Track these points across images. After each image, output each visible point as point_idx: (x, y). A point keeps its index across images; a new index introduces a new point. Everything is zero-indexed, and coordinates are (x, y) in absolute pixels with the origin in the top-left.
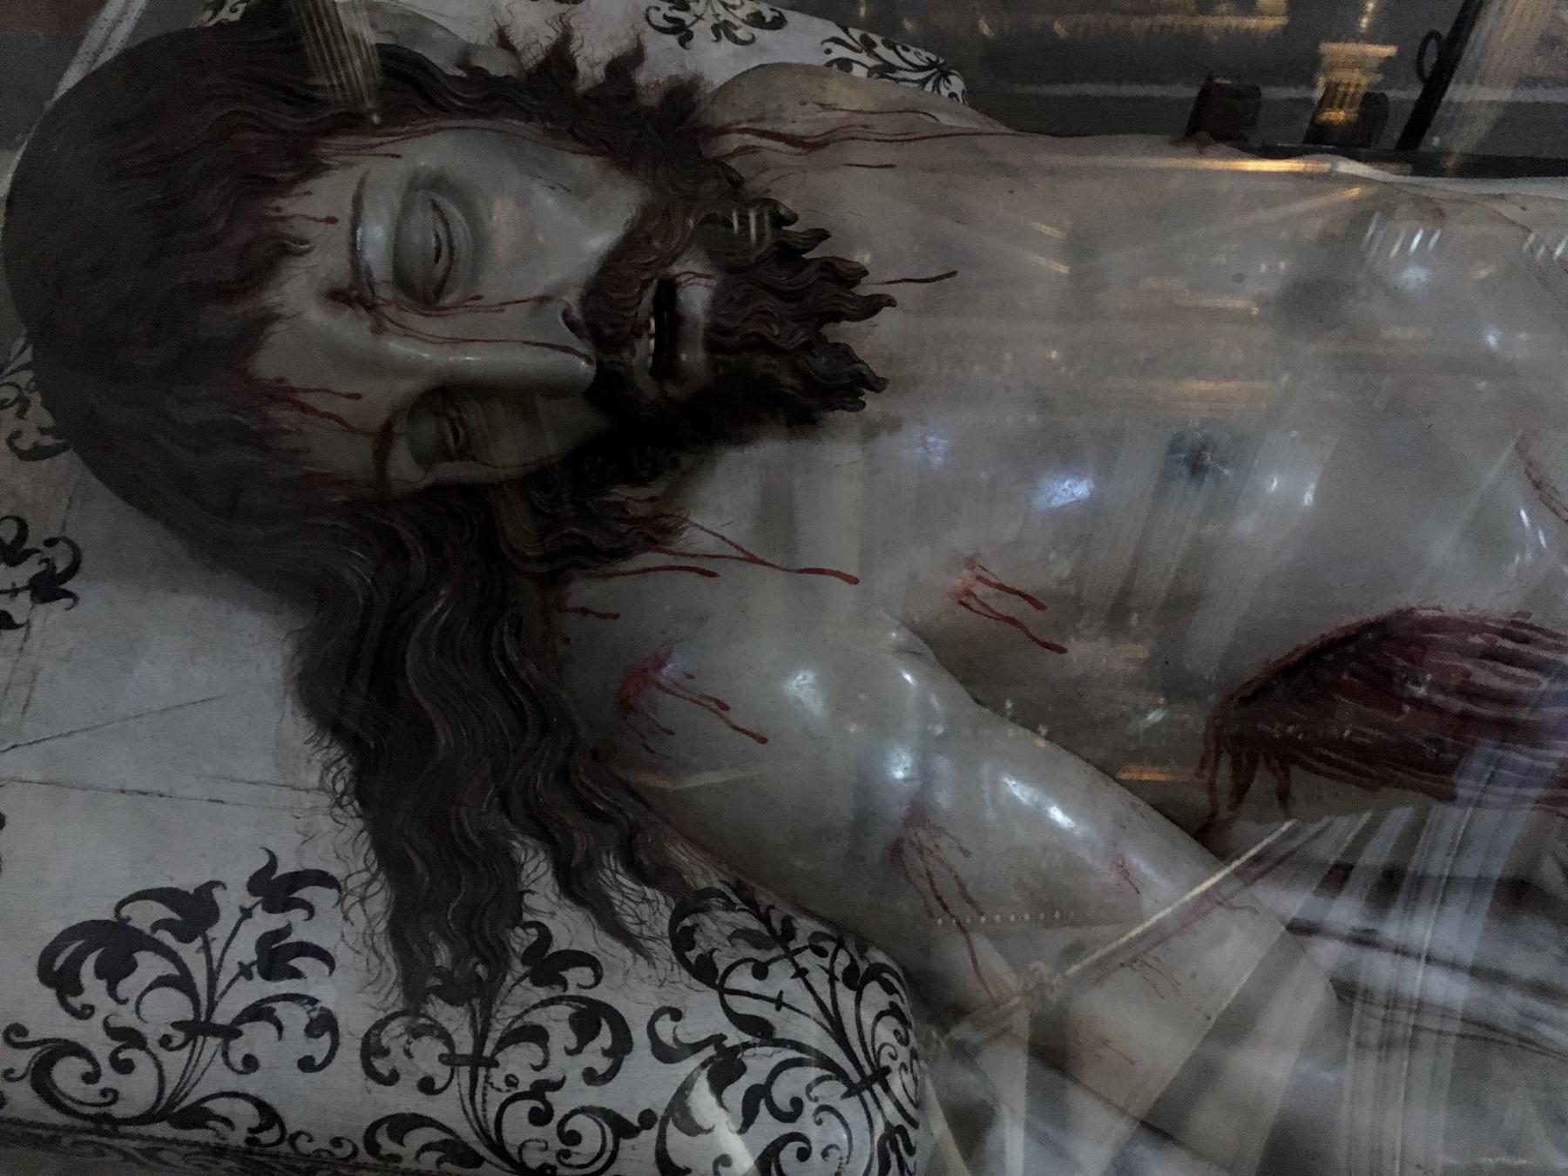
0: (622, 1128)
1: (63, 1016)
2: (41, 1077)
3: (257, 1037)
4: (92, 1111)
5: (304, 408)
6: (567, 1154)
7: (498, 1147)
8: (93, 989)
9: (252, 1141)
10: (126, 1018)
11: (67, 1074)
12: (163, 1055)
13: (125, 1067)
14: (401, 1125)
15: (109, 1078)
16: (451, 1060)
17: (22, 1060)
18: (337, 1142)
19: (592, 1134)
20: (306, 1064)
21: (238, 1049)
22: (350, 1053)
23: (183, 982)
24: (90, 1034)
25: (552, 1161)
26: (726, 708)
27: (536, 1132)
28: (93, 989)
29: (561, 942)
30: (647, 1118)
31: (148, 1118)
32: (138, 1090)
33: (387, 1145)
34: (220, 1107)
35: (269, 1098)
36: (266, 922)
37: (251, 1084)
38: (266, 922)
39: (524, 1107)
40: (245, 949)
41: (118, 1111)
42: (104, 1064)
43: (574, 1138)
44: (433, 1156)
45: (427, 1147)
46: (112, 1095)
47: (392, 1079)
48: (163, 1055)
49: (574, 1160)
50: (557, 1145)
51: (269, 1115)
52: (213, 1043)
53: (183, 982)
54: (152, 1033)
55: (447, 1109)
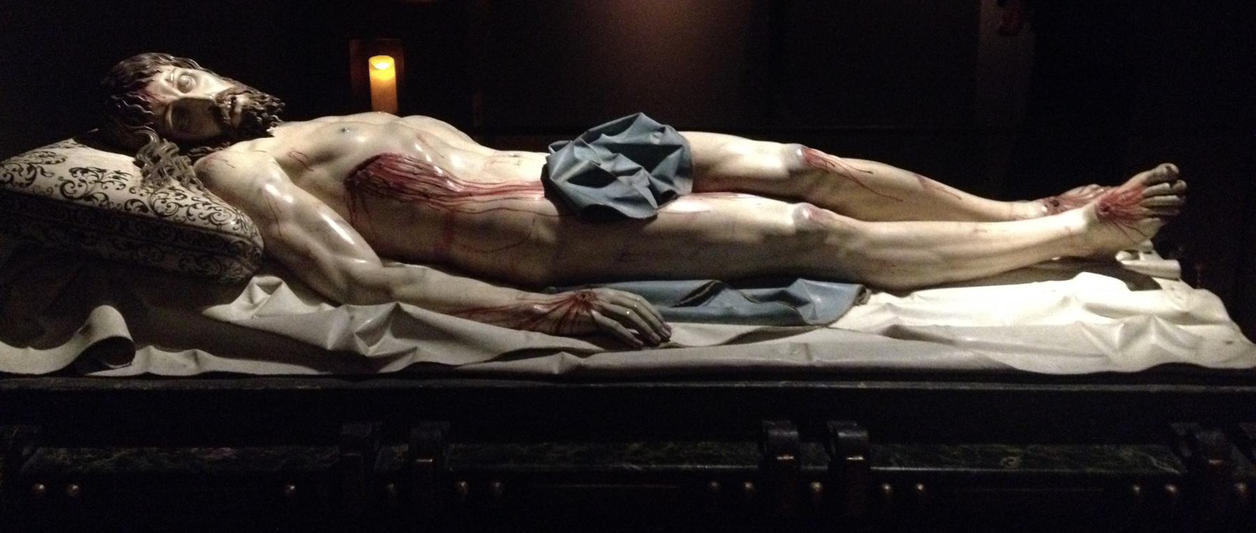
0: (180, 206)
1: (71, 176)
2: (62, 188)
3: (109, 185)
4: (68, 195)
5: (154, 98)
6: (167, 210)
7: (152, 207)
8: (79, 173)
9: (101, 205)
10: (84, 178)
11: (68, 188)
12: (89, 184)
13: (80, 186)
14: (133, 201)
15: (77, 188)
16: (148, 192)
17: (60, 183)
18: (119, 205)
19: (173, 206)
20: (118, 189)
21: (104, 186)
22: (127, 190)
23: (97, 176)
24: (76, 181)
25: (163, 210)
26: (227, 161)
27: (162, 205)
28: (79, 173)
29: (177, 188)
30: (186, 206)
31: (80, 198)
32: (81, 191)
33: (129, 205)
34: (96, 195)
35: (107, 194)
36: (115, 174)
37: (105, 191)
38: (115, 174)
39: (161, 200)
40: (111, 175)
41: (75, 196)
42: (76, 184)
43: (169, 207)
44: (138, 209)
45: (138, 207)
46: (75, 191)
47: (135, 193)
48: (89, 184)
49: (168, 211)
50: (166, 207)
51: (106, 197)
52: (100, 184)
53: (97, 176)
54: (87, 181)
55: (145, 199)
